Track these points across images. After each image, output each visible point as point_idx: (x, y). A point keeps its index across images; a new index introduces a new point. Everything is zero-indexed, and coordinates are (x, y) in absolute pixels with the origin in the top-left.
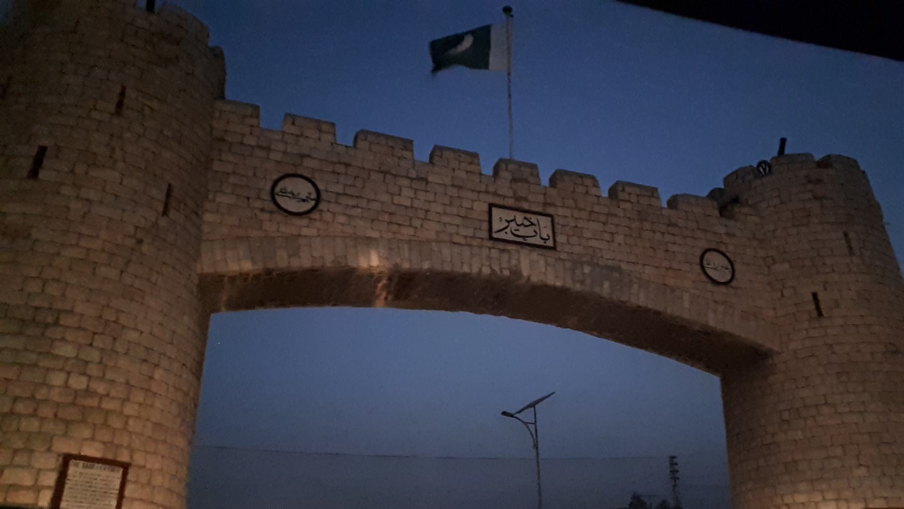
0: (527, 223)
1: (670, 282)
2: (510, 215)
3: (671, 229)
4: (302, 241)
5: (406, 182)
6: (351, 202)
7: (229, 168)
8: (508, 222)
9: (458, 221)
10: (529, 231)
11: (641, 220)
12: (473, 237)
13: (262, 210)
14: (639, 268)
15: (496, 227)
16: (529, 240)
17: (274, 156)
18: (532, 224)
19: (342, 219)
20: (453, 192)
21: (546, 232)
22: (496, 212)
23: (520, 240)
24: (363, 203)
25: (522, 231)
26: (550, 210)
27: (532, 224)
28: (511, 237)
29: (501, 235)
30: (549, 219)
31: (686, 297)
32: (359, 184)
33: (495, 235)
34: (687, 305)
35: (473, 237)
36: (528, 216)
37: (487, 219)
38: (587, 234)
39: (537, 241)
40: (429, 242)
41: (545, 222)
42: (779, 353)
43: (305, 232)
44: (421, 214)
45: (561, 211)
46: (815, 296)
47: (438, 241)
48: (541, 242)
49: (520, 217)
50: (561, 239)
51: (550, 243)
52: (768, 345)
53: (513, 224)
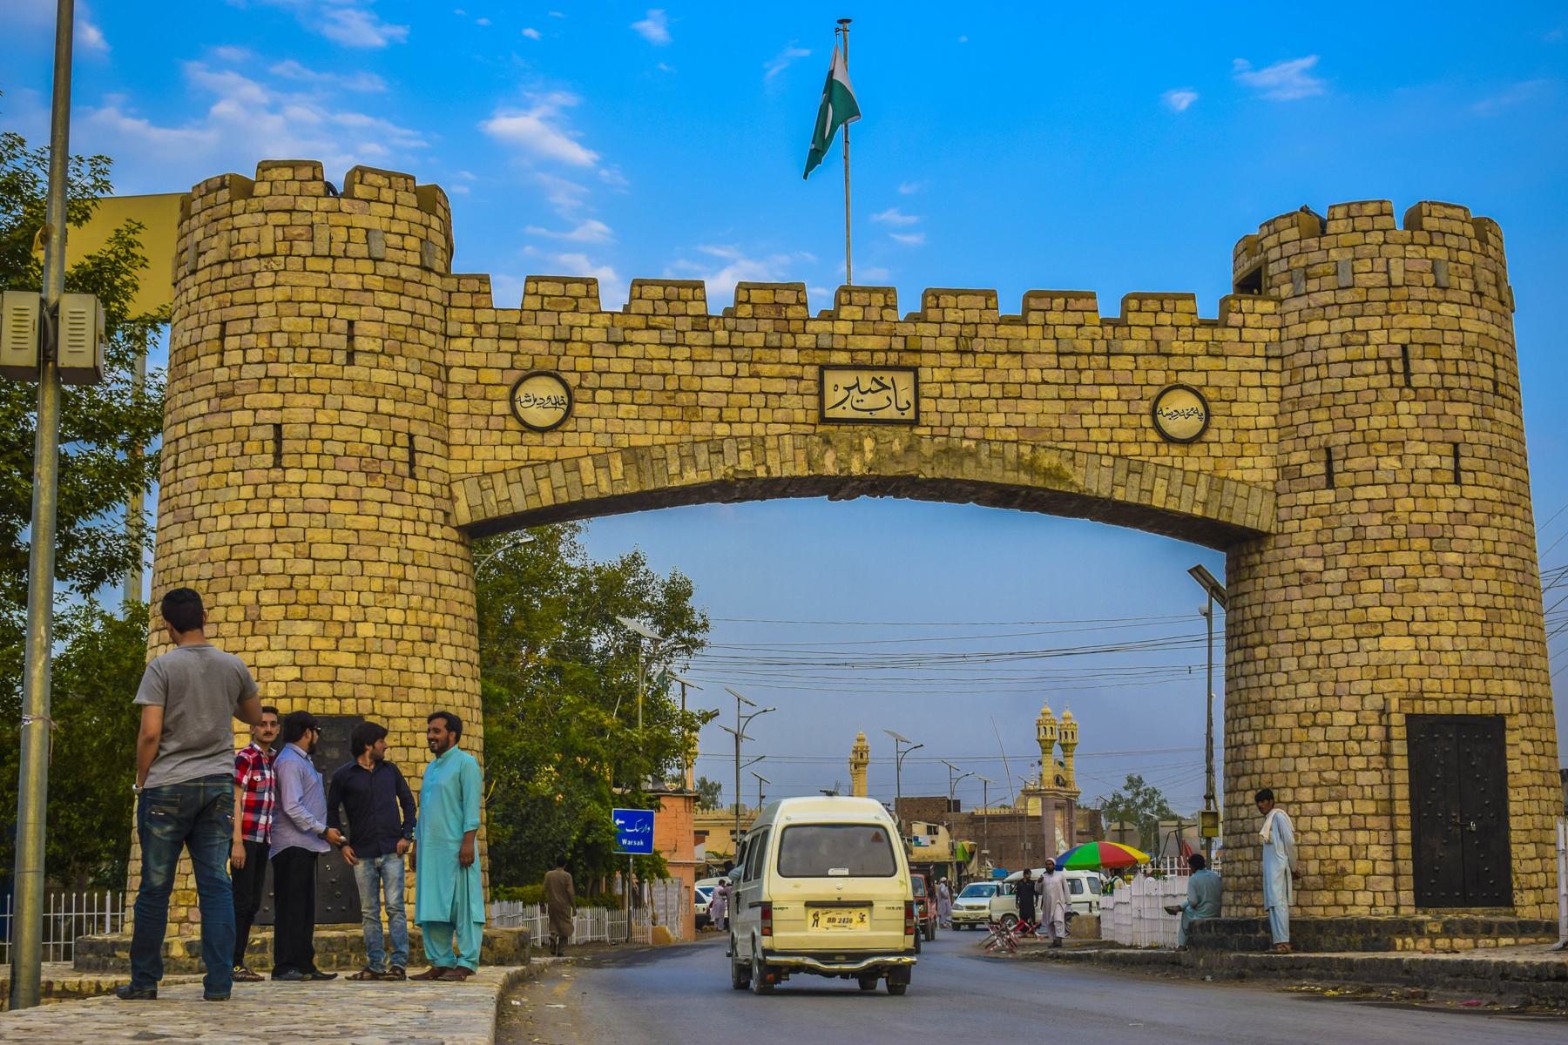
0: (876, 387)
2: (848, 378)
8: (848, 389)
10: (880, 399)
15: (828, 404)
16: (878, 415)
18: (885, 387)
21: (906, 395)
22: (831, 378)
23: (866, 415)
25: (870, 401)
26: (910, 359)
27: (885, 387)
28: (850, 413)
29: (838, 413)
30: (911, 375)
33: (829, 414)
36: (877, 375)
37: (815, 390)
39: (891, 413)
41: (904, 381)
45: (929, 359)
48: (896, 415)
49: (866, 379)
50: (926, 405)
51: (909, 415)
52: (1250, 522)
53: (855, 392)
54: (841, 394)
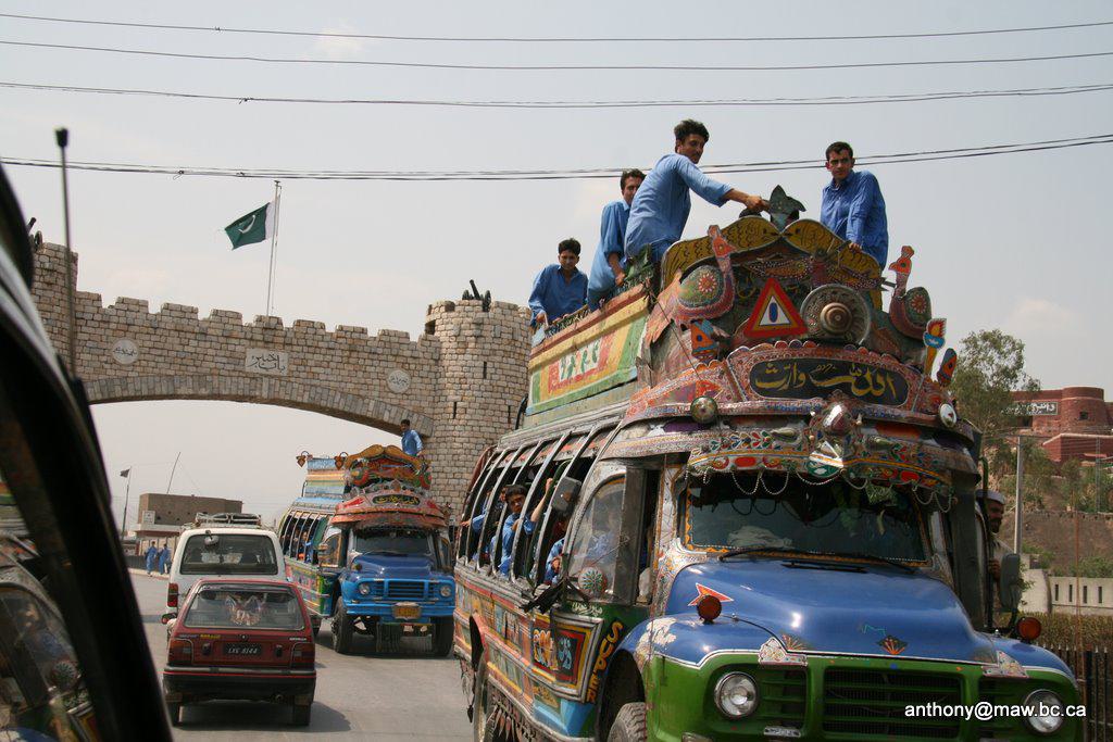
1: (362, 393)
3: (371, 356)
4: (129, 380)
5: (193, 336)
6: (159, 352)
7: (86, 337)
9: (225, 360)
11: (351, 351)
12: (234, 370)
13: (106, 362)
14: (343, 385)
17: (113, 326)
19: (153, 364)
20: (222, 340)
24: (165, 353)
31: (372, 403)
32: (163, 339)
34: (371, 407)
35: (234, 370)
38: (310, 363)
40: (205, 375)
42: (428, 437)
43: (130, 374)
44: (201, 357)
46: (455, 403)
47: (212, 375)
54: (255, 360)
